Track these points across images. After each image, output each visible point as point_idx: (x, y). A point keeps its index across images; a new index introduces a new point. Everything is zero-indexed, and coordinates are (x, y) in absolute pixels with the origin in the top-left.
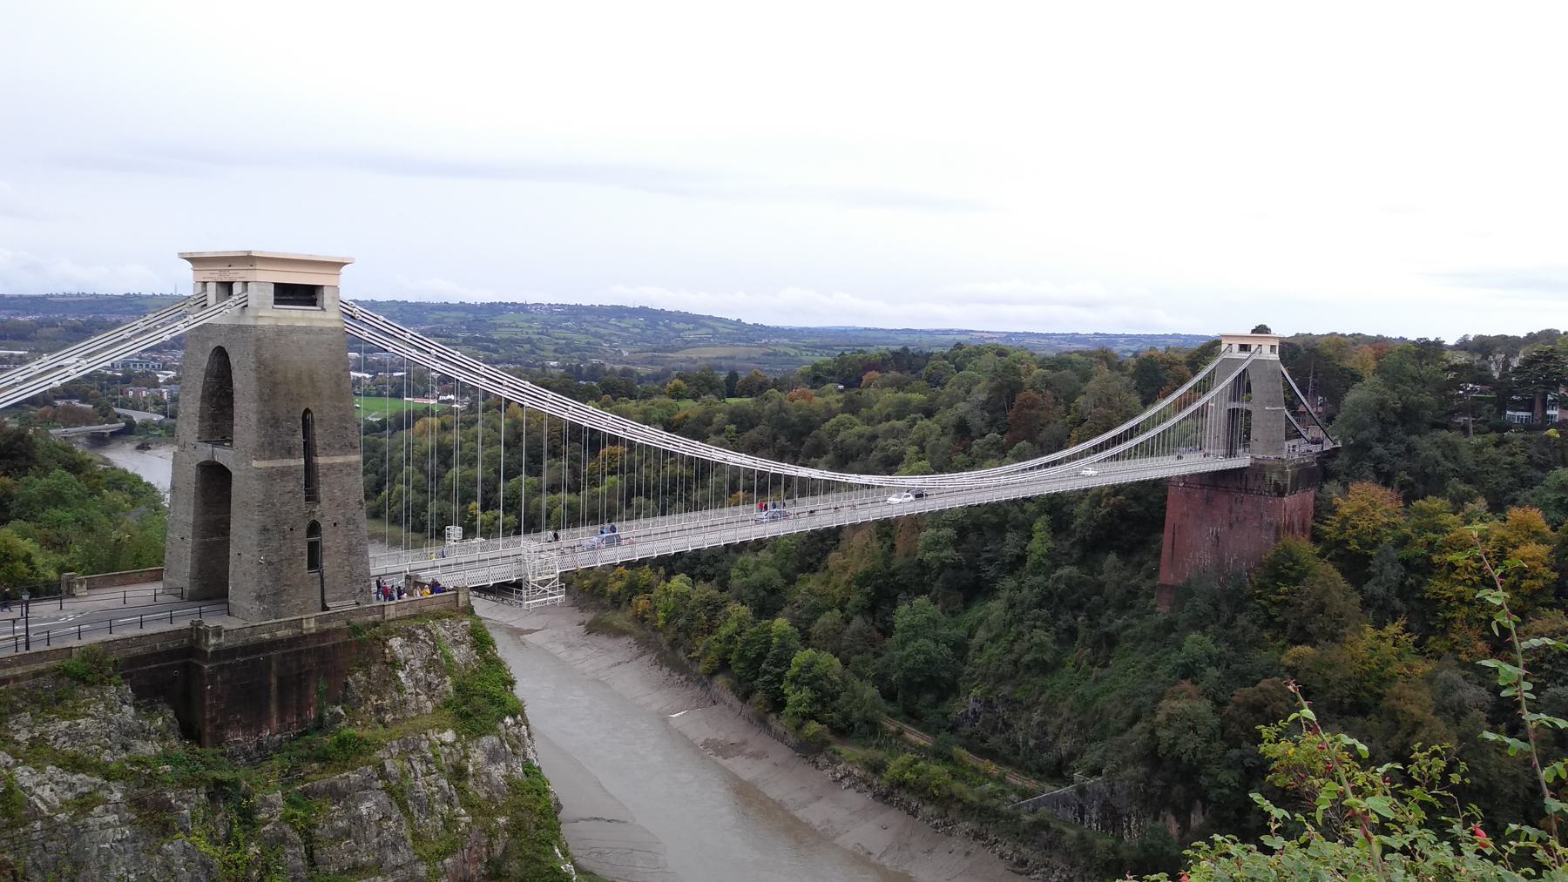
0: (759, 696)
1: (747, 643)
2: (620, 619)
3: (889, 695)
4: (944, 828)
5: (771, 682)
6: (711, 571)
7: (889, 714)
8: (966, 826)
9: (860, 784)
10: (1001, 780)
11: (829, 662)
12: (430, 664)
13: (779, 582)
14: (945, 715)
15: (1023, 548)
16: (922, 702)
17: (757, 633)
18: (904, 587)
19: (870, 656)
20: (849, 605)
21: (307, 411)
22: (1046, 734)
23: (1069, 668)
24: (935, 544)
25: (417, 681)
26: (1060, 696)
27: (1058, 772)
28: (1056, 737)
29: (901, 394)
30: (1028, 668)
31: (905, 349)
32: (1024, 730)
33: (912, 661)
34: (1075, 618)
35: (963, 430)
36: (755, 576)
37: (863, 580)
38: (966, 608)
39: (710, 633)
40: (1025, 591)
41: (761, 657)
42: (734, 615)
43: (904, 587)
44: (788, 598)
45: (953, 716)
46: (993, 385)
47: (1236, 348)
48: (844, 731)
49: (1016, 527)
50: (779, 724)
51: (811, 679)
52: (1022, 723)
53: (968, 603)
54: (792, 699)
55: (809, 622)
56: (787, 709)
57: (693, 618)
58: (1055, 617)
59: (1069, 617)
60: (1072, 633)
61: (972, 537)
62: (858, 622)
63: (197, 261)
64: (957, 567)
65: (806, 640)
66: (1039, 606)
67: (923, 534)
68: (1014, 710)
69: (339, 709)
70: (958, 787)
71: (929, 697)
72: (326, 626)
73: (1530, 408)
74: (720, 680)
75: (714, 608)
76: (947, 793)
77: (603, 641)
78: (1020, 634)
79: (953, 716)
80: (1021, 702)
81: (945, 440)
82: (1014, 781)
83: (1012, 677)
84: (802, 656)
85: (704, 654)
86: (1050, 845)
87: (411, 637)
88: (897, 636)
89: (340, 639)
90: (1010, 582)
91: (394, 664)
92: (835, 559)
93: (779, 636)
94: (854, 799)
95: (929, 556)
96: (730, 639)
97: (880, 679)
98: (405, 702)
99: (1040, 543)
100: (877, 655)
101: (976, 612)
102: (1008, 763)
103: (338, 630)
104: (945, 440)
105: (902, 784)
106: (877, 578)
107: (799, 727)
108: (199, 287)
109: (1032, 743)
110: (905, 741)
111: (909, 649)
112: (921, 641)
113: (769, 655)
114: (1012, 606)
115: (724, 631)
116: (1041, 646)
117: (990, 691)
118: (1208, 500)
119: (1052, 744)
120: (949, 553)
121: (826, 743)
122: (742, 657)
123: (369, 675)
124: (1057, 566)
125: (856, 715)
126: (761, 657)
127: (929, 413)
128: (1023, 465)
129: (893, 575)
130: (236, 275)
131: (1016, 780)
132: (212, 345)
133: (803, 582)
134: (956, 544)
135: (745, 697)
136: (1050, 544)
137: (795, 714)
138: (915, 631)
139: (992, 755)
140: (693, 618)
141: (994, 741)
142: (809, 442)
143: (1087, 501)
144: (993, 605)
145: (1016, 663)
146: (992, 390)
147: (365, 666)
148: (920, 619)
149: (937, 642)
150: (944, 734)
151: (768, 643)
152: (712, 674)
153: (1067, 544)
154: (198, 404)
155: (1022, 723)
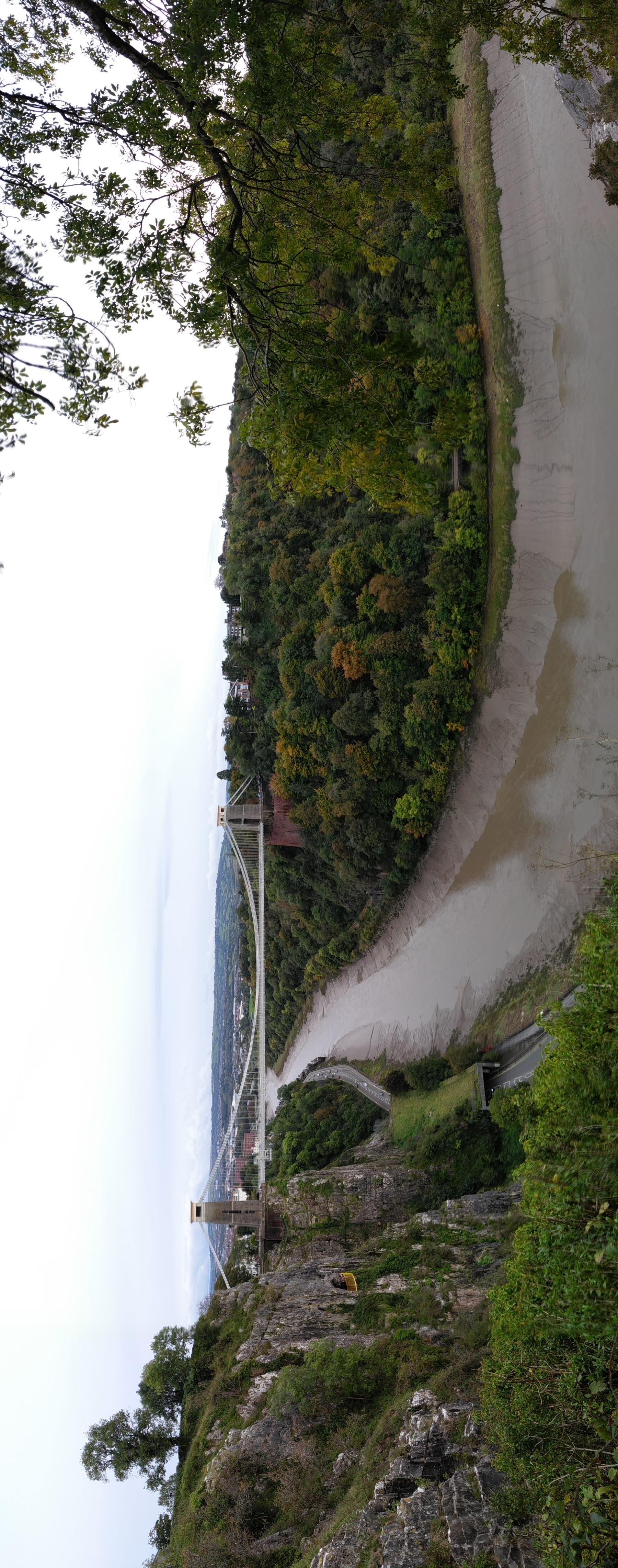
2: (321, 983)
4: (385, 930)
8: (384, 925)
9: (371, 947)
24: (293, 901)
48: (355, 944)
60: (321, 874)
75: (315, 963)
77: (328, 991)
86: (389, 907)
94: (375, 950)
105: (371, 938)
118: (276, 834)
126: (331, 961)
139: (363, 906)
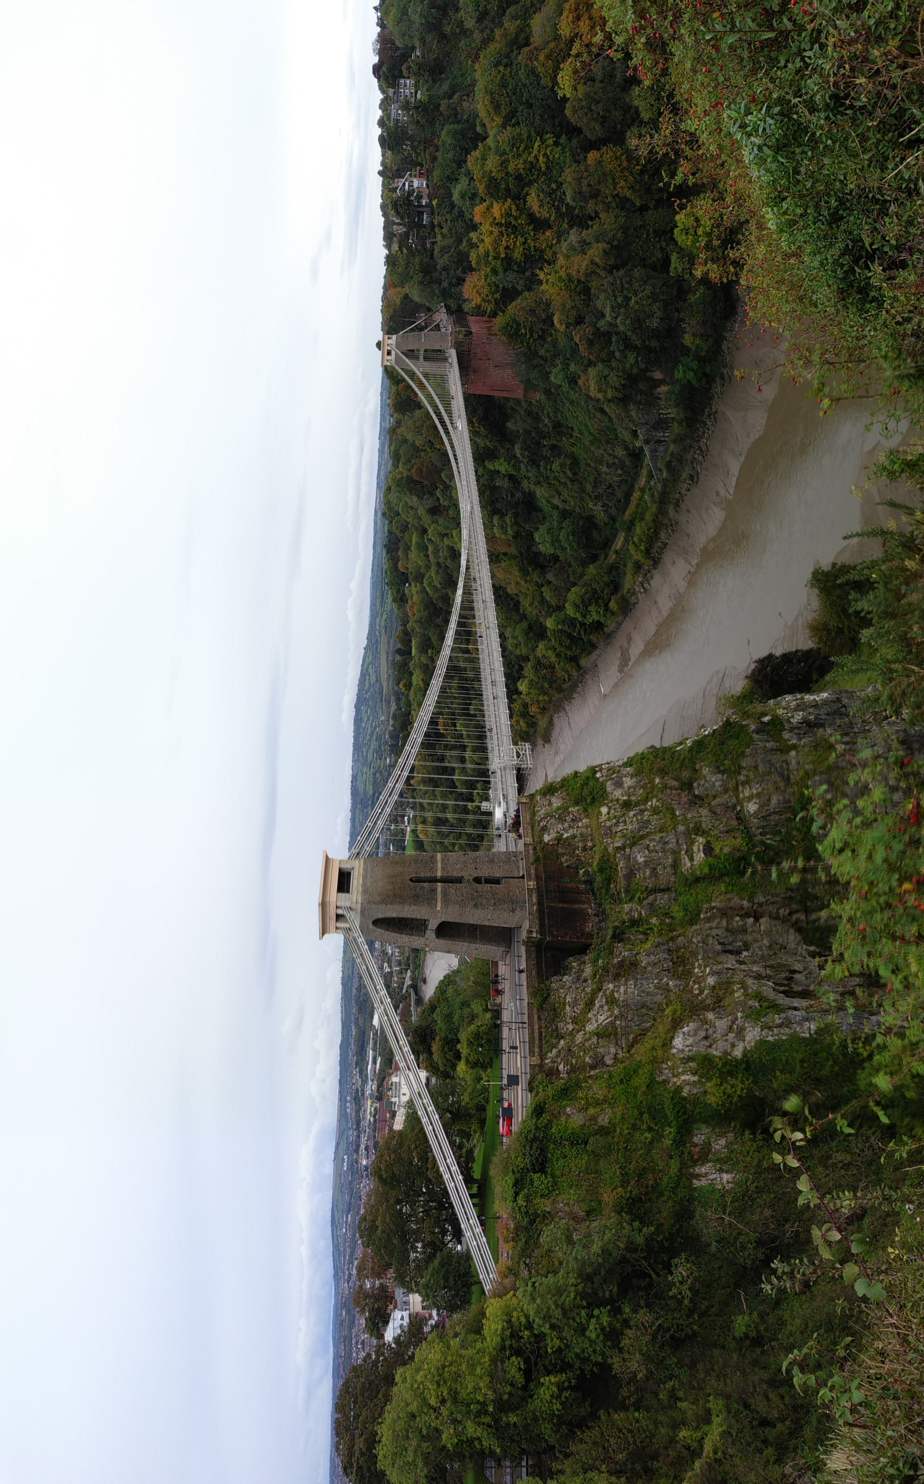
0: (593, 638)
1: (561, 644)
3: (594, 558)
5: (585, 630)
6: (517, 667)
7: (605, 559)
10: (643, 490)
11: (574, 594)
12: (561, 820)
13: (525, 624)
14: (606, 524)
15: (505, 476)
16: (598, 538)
17: (555, 638)
18: (529, 548)
19: (570, 569)
20: (540, 582)
22: (614, 464)
23: (574, 449)
24: (503, 528)
25: (570, 827)
26: (591, 455)
27: (636, 456)
28: (615, 457)
29: (412, 548)
30: (575, 474)
32: (613, 477)
33: (573, 544)
34: (545, 446)
35: (435, 511)
36: (521, 639)
37: (525, 572)
38: (541, 510)
39: (554, 668)
40: (530, 475)
41: (570, 636)
42: (544, 652)
43: (529, 548)
44: (535, 619)
45: (606, 520)
46: (408, 493)
48: (616, 587)
49: (493, 480)
50: (610, 625)
51: (584, 606)
52: (608, 478)
53: (539, 510)
54: (595, 617)
55: (550, 606)
56: (602, 620)
57: (544, 678)
58: (545, 458)
59: (544, 449)
60: (553, 448)
61: (498, 506)
62: (550, 576)
64: (516, 515)
65: (560, 608)
66: (539, 466)
67: (497, 535)
68: (601, 482)
69: (581, 872)
70: (648, 517)
71: (595, 533)
72: (533, 876)
73: (422, 213)
74: (583, 662)
75: (539, 665)
76: (652, 524)
78: (555, 478)
79: (606, 520)
80: (596, 478)
81: (441, 521)
82: (643, 483)
83: (581, 483)
84: (570, 611)
85: (567, 671)
87: (544, 829)
88: (558, 552)
89: (541, 868)
90: (525, 484)
91: (559, 839)
92: (511, 590)
93: (557, 624)
95: (510, 532)
96: (558, 655)
97: (584, 564)
98: (581, 834)
99: (502, 466)
100: (570, 565)
101: (543, 504)
102: (632, 486)
103: (536, 870)
104: (441, 521)
105: (648, 552)
106: (523, 564)
107: (613, 613)
109: (620, 472)
110: (621, 549)
111: (566, 545)
112: (561, 538)
113: (569, 631)
114: (539, 483)
115: (553, 659)
116: (562, 466)
117: (590, 496)
119: (620, 460)
120: (508, 519)
121: (623, 597)
122: (569, 648)
123: (564, 854)
124: (515, 457)
125: (606, 579)
126: (570, 636)
127: (425, 531)
128: (456, 473)
129: (521, 554)
131: (642, 481)
133: (525, 610)
134: (502, 515)
135: (594, 647)
136: (502, 460)
137: (604, 616)
138: (555, 541)
139: (628, 496)
140: (544, 678)
141: (619, 494)
142: (440, 605)
143: (477, 439)
144: (538, 494)
145: (572, 481)
146: (411, 493)
147: (558, 856)
148: (548, 538)
149: (562, 528)
150: (617, 525)
151: (561, 631)
152: (579, 667)
153: (502, 451)
155: (608, 478)
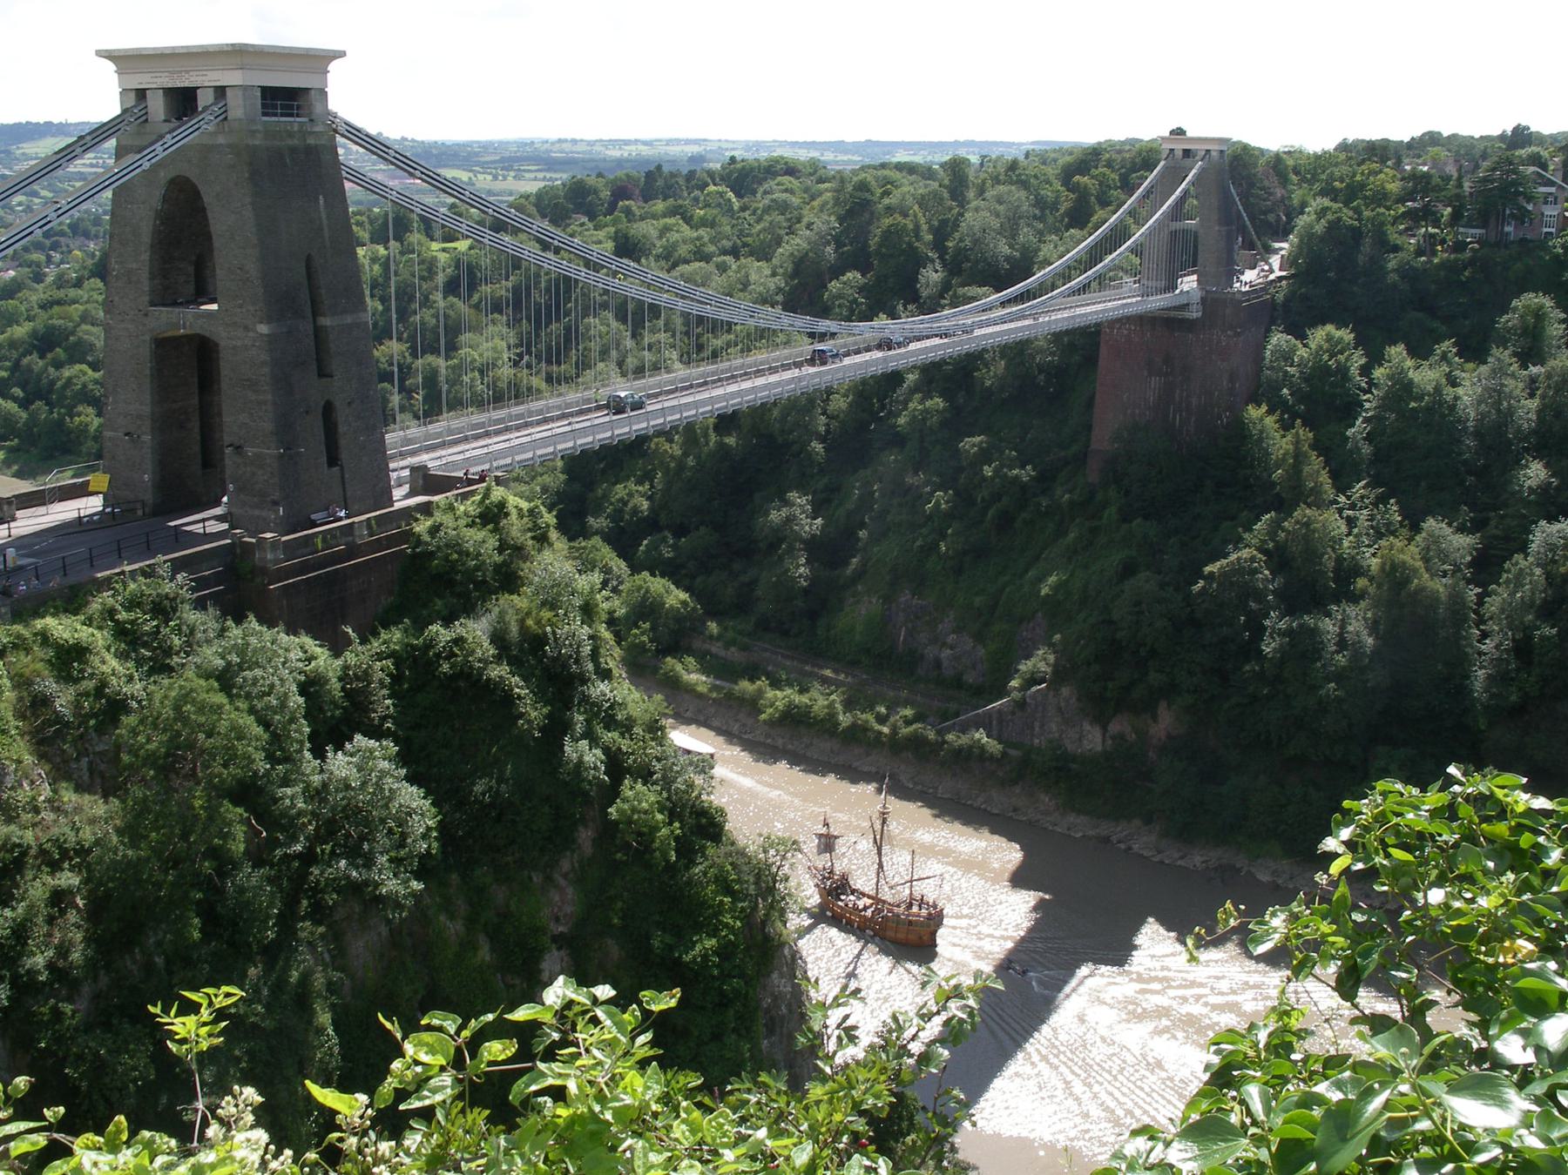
21: (309, 259)
31: (659, 167)
47: (1179, 154)
63: (124, 60)
108: (133, 95)
130: (204, 79)
132: (164, 176)
154: (146, 256)
